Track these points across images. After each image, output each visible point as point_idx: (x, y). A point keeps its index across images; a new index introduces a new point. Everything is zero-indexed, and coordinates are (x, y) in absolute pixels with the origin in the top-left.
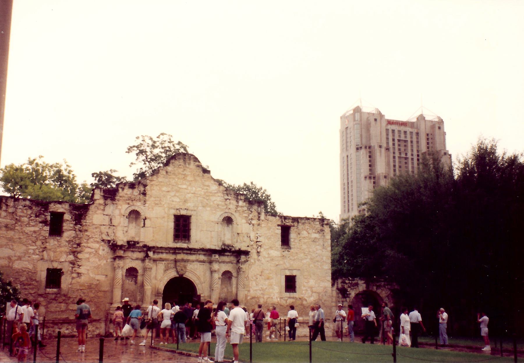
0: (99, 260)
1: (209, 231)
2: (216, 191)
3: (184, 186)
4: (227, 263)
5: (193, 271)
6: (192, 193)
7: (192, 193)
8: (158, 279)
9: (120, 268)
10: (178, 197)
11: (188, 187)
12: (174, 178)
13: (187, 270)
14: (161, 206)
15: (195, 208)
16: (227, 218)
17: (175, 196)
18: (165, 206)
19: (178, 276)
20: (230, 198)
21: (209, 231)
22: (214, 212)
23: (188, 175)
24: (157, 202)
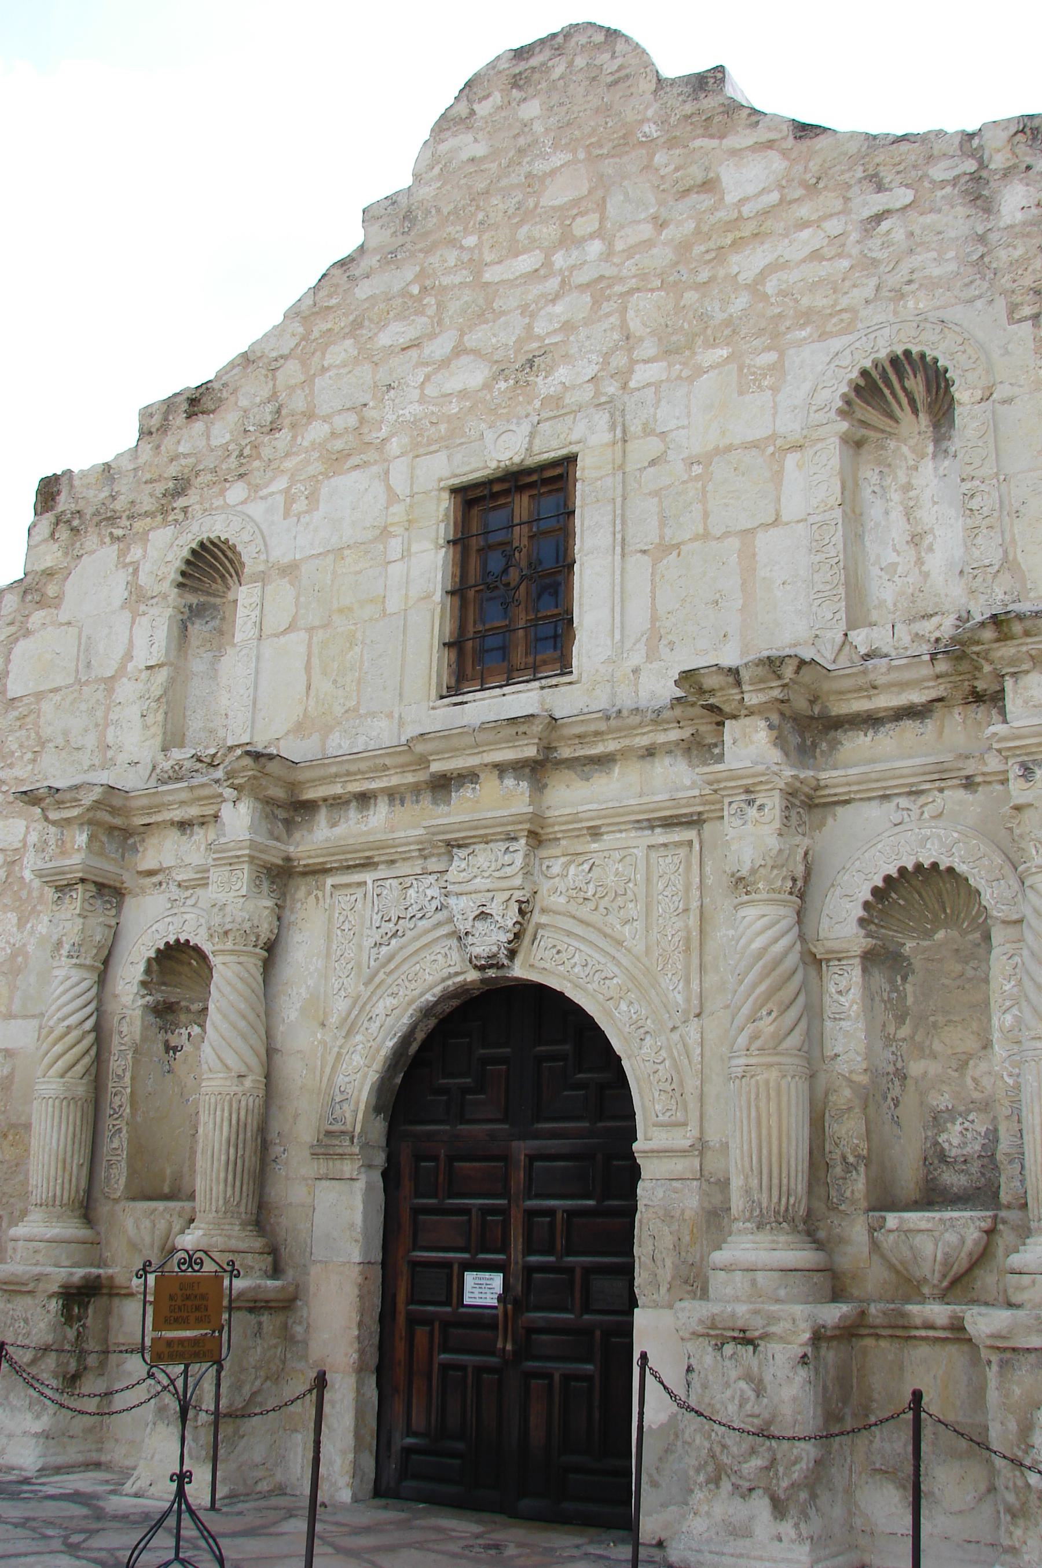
0: (21, 924)
1: (727, 534)
2: (774, 197)
3: (526, 263)
4: (915, 793)
5: (595, 918)
6: (583, 287)
7: (583, 287)
8: (334, 1020)
9: (64, 952)
10: (476, 352)
11: (548, 256)
12: (452, 242)
13: (544, 919)
14: (366, 464)
15: (611, 388)
16: (916, 384)
17: (459, 351)
18: (394, 446)
19: (473, 975)
20: (905, 196)
21: (727, 534)
22: (771, 357)
23: (553, 173)
24: (339, 445)
